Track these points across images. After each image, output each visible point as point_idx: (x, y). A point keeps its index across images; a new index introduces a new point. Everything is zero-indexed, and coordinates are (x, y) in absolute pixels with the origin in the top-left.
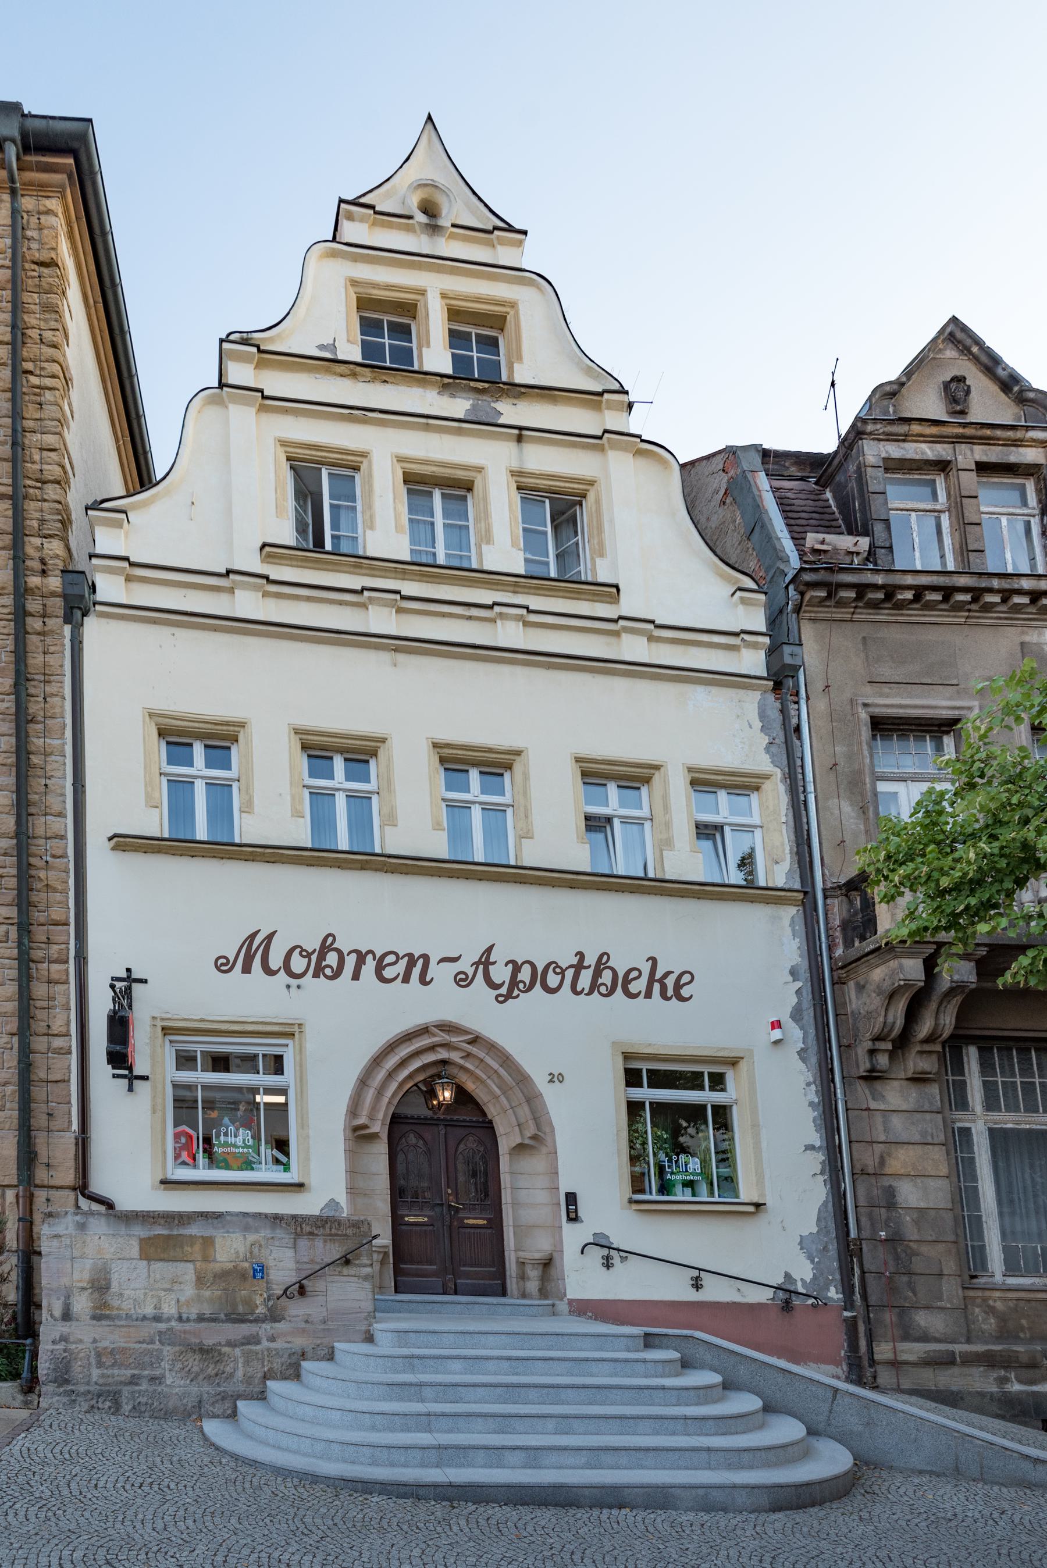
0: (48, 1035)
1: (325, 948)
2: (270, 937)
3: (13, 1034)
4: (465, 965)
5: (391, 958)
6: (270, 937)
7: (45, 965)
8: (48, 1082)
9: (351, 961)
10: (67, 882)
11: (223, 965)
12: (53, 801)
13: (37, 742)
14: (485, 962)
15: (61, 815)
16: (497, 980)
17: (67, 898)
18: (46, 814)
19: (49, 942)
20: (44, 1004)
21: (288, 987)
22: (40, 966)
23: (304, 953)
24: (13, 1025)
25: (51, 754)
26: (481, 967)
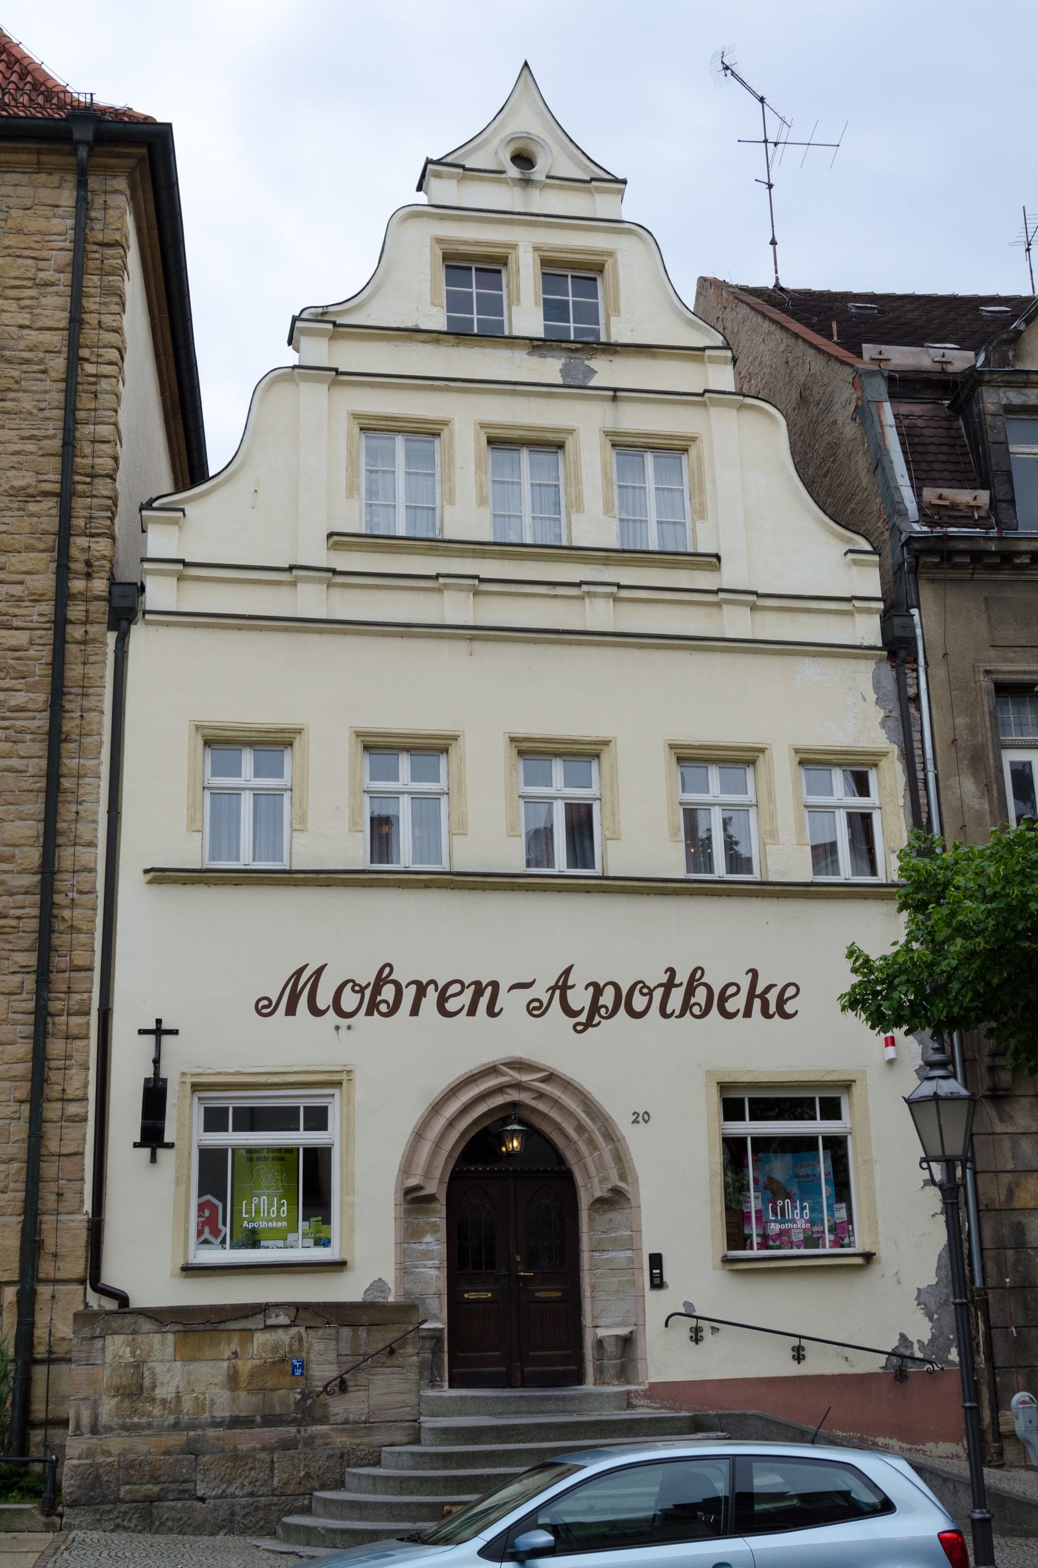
0: (63, 1100)
1: (380, 981)
2: (319, 972)
3: (21, 1102)
4: (539, 991)
5: (455, 988)
6: (319, 972)
7: (64, 1018)
8: (60, 1155)
9: (409, 995)
10: (93, 921)
11: (264, 1008)
12: (83, 829)
13: (70, 764)
14: (562, 986)
15: (92, 844)
16: (576, 1007)
17: (93, 939)
18: (75, 845)
19: (69, 991)
20: (60, 1064)
21: (337, 1028)
22: (57, 1019)
23: (357, 988)
24: (24, 1090)
25: (85, 776)
26: (558, 992)
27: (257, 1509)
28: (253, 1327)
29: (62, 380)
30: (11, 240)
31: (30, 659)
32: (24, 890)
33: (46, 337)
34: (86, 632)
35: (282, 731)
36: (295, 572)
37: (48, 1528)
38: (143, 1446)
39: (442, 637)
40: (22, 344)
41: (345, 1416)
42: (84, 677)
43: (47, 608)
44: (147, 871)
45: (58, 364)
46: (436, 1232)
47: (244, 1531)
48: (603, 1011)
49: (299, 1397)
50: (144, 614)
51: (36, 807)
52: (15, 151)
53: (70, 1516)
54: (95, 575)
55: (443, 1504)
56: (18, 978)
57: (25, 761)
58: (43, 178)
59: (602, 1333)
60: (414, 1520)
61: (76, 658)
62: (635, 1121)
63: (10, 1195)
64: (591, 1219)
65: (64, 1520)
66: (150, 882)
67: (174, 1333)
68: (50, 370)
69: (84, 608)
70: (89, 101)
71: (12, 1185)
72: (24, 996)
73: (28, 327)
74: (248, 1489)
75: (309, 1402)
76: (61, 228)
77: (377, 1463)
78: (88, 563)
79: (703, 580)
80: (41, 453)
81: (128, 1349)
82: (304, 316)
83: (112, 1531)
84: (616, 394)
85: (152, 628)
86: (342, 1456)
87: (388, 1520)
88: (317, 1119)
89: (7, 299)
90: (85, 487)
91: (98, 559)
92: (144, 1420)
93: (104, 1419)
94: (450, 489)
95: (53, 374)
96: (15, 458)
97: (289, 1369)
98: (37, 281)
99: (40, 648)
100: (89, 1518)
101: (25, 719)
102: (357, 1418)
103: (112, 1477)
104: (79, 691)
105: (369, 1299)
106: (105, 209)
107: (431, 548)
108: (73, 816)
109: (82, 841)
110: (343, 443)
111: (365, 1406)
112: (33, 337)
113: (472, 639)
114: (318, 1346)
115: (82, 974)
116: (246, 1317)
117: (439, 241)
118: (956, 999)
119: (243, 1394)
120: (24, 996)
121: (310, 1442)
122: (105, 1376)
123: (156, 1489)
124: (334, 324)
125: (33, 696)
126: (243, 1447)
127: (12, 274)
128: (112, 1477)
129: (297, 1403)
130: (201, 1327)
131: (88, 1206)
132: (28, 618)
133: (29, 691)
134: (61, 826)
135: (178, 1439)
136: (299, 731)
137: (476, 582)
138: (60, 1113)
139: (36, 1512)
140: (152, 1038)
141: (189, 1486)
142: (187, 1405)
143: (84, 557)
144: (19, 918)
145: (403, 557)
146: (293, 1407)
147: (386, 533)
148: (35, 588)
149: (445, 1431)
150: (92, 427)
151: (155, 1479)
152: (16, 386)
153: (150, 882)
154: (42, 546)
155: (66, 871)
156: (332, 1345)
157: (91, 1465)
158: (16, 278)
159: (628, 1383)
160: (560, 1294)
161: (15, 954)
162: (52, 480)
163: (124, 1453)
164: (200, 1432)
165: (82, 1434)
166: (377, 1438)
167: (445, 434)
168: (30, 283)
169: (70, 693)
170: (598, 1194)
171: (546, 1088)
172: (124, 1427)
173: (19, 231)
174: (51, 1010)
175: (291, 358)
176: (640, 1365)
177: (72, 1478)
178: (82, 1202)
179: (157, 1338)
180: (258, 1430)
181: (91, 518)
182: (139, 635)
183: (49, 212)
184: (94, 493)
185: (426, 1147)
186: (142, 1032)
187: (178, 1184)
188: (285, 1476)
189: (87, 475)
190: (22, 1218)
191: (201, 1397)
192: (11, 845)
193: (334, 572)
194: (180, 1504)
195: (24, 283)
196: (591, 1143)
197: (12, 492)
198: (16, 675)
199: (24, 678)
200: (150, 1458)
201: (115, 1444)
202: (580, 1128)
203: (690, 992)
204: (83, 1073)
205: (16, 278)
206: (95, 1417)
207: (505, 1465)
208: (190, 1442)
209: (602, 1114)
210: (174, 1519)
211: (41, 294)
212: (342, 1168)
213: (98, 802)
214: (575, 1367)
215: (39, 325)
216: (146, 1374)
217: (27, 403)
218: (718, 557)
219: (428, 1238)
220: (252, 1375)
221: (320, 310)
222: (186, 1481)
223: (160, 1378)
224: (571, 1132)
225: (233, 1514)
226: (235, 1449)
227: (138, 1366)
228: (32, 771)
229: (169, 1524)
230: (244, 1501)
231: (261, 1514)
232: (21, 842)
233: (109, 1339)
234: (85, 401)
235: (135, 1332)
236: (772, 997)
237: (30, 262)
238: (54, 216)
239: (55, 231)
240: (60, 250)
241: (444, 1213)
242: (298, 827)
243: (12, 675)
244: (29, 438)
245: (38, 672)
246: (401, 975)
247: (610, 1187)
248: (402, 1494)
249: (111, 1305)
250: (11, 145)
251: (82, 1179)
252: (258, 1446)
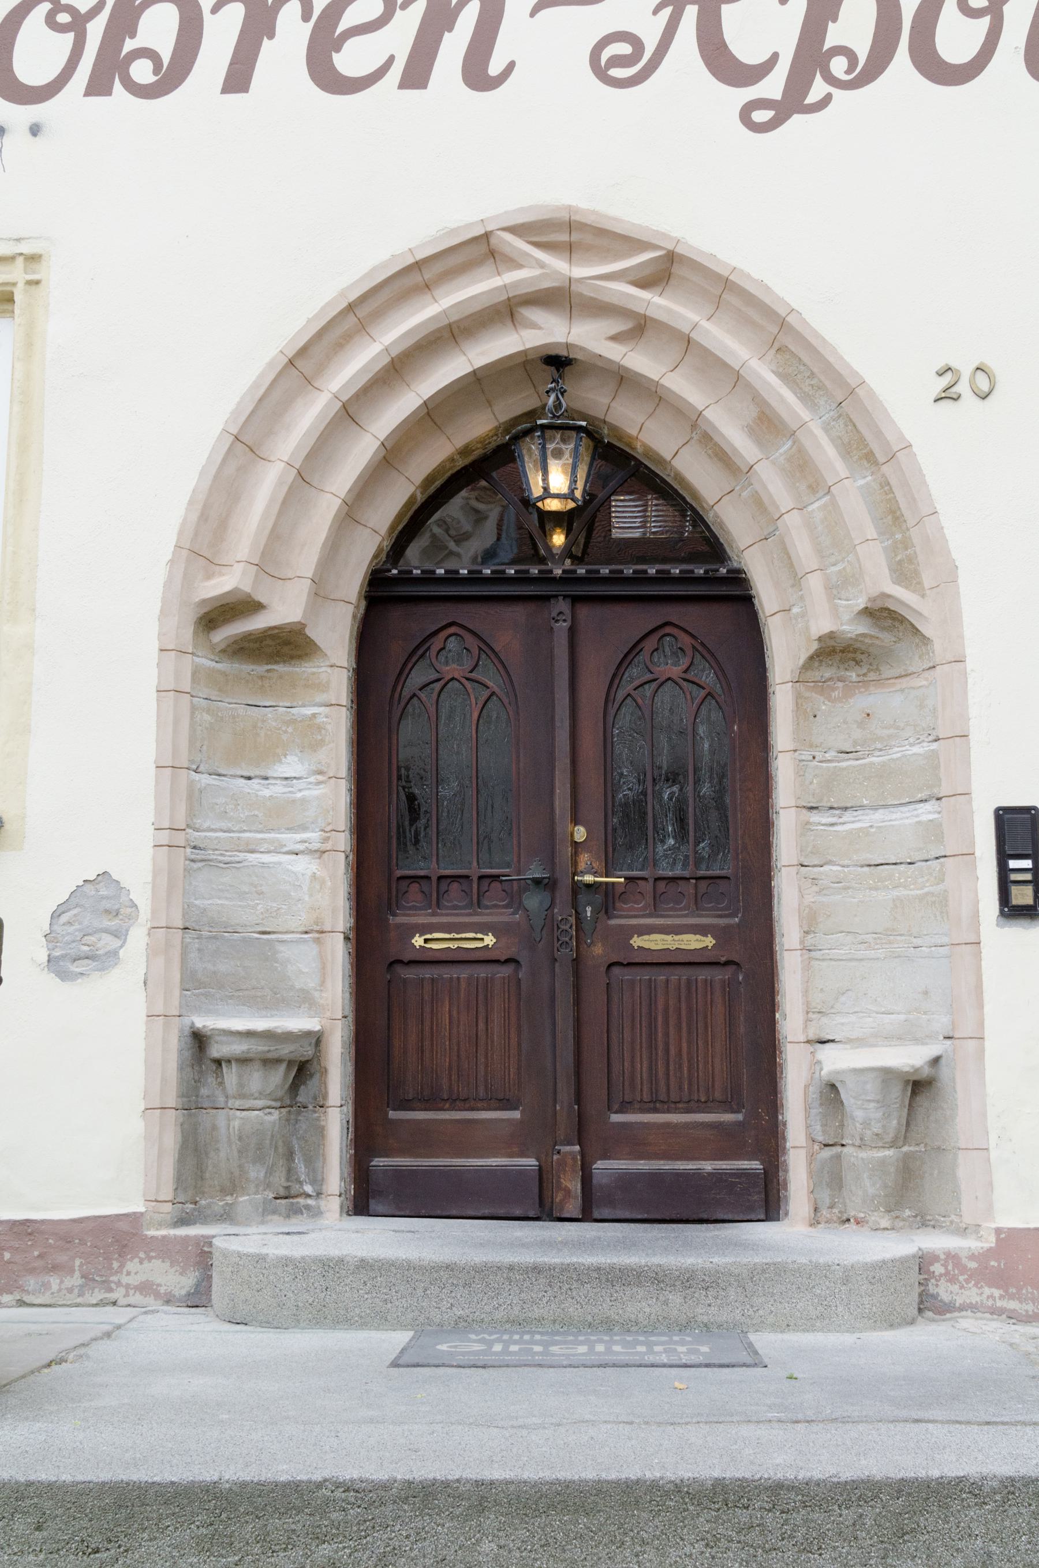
46: (315, 746)
48: (838, 66)
62: (948, 396)
64: (803, 713)
159: (924, 1221)
160: (709, 941)
170: (823, 625)
176: (966, 1168)
209: (839, 379)
219: (292, 765)
247: (861, 603)
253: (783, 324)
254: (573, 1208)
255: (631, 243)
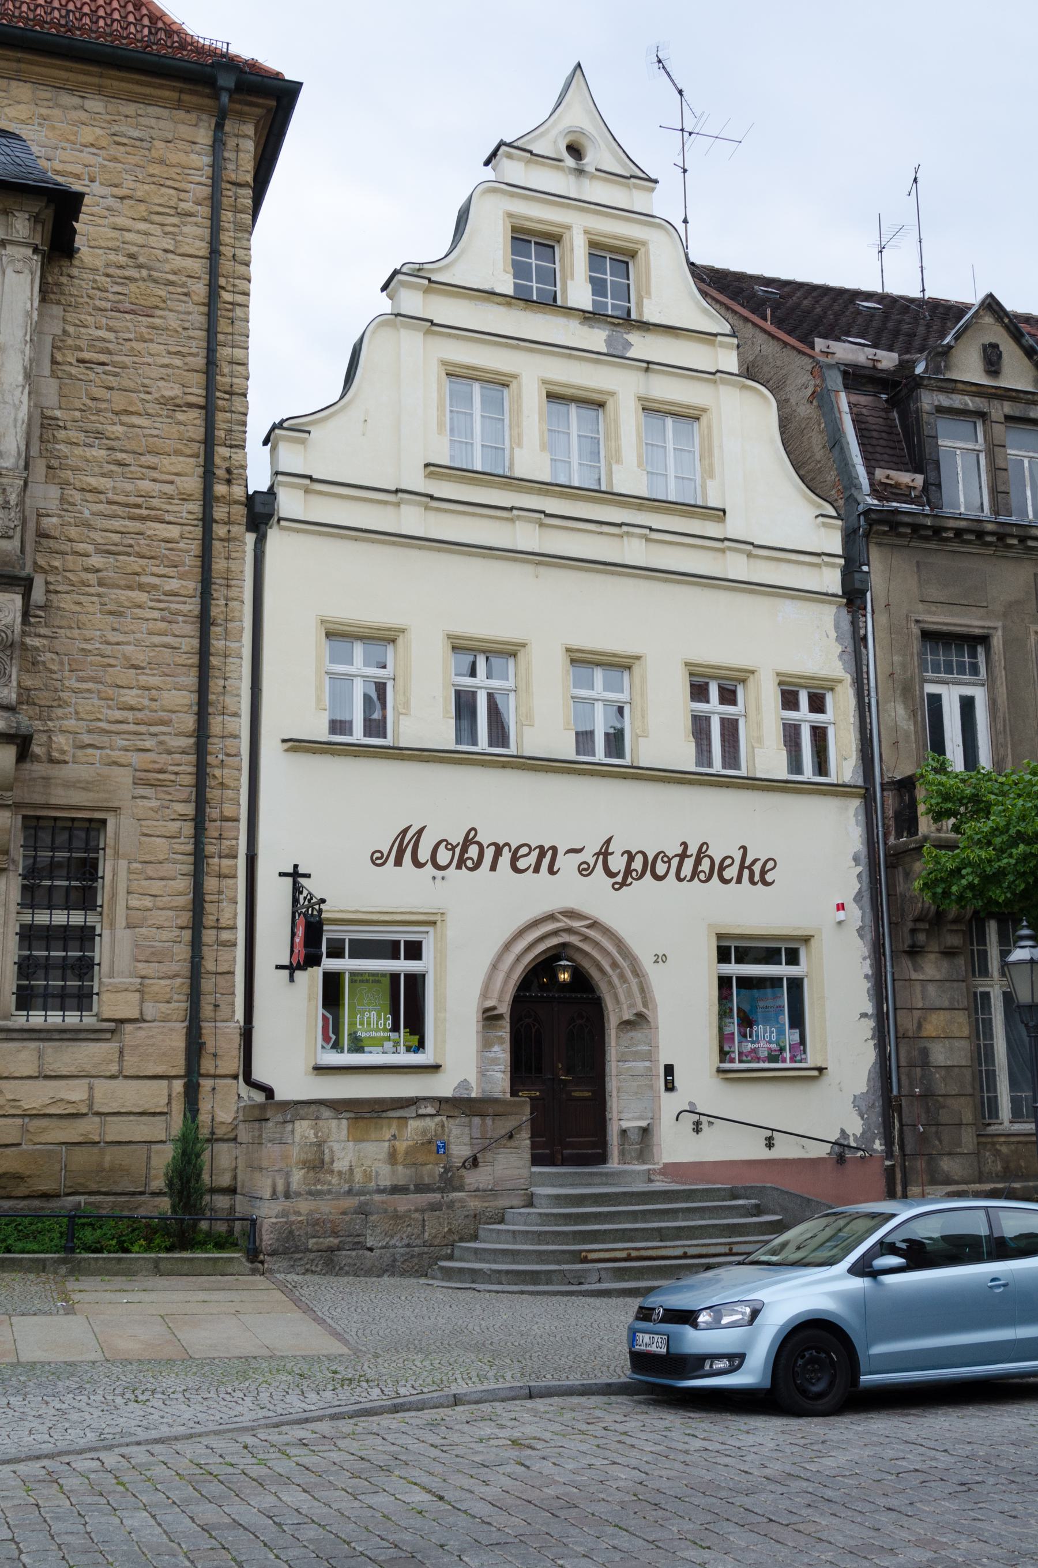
0: (218, 928)
1: (467, 842)
2: (420, 832)
3: (182, 928)
4: (588, 856)
5: (524, 850)
6: (420, 832)
7: (216, 860)
8: (216, 973)
9: (489, 853)
10: (239, 780)
11: (378, 859)
12: (229, 700)
13: (217, 644)
14: (604, 853)
15: (236, 715)
16: (614, 870)
17: (239, 794)
18: (223, 714)
19: (220, 837)
20: (215, 898)
21: (434, 878)
22: (210, 861)
23: (449, 847)
24: (185, 918)
25: (229, 656)
26: (601, 857)
27: (413, 1256)
28: (408, 1116)
29: (204, 304)
30: (154, 169)
31: (181, 551)
32: (181, 750)
33: (189, 263)
34: (229, 531)
35: (389, 629)
36: (400, 495)
37: (254, 1272)
38: (326, 1208)
39: (515, 560)
40: (167, 267)
41: (476, 1185)
42: (228, 570)
43: (196, 507)
44: (284, 741)
45: (200, 289)
46: (502, 1043)
47: (403, 1274)
48: (634, 874)
49: (442, 1170)
50: (279, 520)
51: (191, 679)
52: (161, 87)
53: (270, 1263)
54: (234, 482)
55: (581, 1251)
56: (178, 824)
57: (179, 640)
58: (181, 114)
59: (625, 1125)
60: (559, 1263)
61: (220, 553)
62: (656, 962)
63: (174, 1005)
64: (618, 1037)
65: (266, 1266)
66: (286, 750)
67: (347, 1119)
68: (192, 294)
69: (227, 510)
70: (225, 50)
71: (176, 997)
72: (182, 840)
73: (172, 252)
74: (406, 1241)
75: (450, 1174)
76: (199, 164)
77: (502, 1221)
78: (229, 471)
79: (711, 529)
80: (186, 368)
81: (312, 1132)
82: (404, 270)
83: (304, 1274)
84: (648, 366)
85: (285, 533)
86: (475, 1216)
87: (538, 1263)
88: (414, 951)
89: (152, 223)
90: (224, 402)
91: (237, 468)
92: (325, 1187)
93: (294, 1187)
94: (519, 434)
95: (195, 298)
96: (163, 370)
97: (435, 1148)
98: (179, 210)
99: (189, 542)
100: (285, 1264)
101: (178, 603)
102: (485, 1187)
103: (302, 1232)
104: (224, 582)
105: (457, 1095)
106: (237, 152)
107: (506, 484)
108: (220, 689)
109: (229, 712)
110: (435, 386)
111: (491, 1178)
112: (178, 262)
113: (539, 563)
114: (456, 1131)
115: (230, 824)
116: (402, 1108)
117: (510, 215)
118: (1009, 887)
119: (400, 1168)
120: (182, 840)
121: (451, 1205)
122: (295, 1153)
123: (336, 1241)
124: (429, 280)
125: (184, 583)
126: (401, 1209)
127: (157, 201)
128: (302, 1232)
129: (441, 1175)
130: (368, 1115)
131: (240, 1015)
132: (179, 515)
133: (180, 579)
134: (212, 697)
135: (351, 1202)
136: (403, 631)
137: (542, 516)
138: (214, 938)
139: (244, 1260)
140: (290, 880)
141: (361, 1239)
142: (358, 1176)
143: (226, 464)
144: (176, 773)
145: (471, 487)
146: (437, 1178)
147: (459, 466)
148: (184, 489)
149: (558, 1197)
150: (230, 349)
151: (335, 1234)
152: (162, 305)
153: (286, 750)
154: (188, 452)
155: (216, 736)
156: (467, 1130)
157: (286, 1223)
158: (160, 205)
159: (644, 1163)
161: (174, 804)
162: (197, 393)
163: (310, 1213)
164: (368, 1197)
165: (277, 1199)
166: (502, 1202)
167: (514, 385)
168: (172, 211)
169: (215, 584)
170: (626, 1017)
171: (591, 933)
172: (310, 1193)
173: (162, 162)
174: (207, 853)
175: (384, 305)
176: (655, 1149)
177: (272, 1232)
178: (234, 1012)
179: (334, 1123)
180: (412, 1196)
181: (231, 431)
182: (275, 538)
183: (187, 147)
184: (233, 409)
185: (500, 977)
186: (282, 874)
187: (310, 1000)
188: (434, 1231)
189: (226, 393)
190: (186, 1024)
191: (369, 1170)
192: (168, 711)
193: (432, 497)
194: (354, 1253)
195: (168, 210)
196: (622, 977)
197: (162, 401)
198: (170, 564)
199: (176, 567)
200: (331, 1217)
201: (304, 1206)
202: (615, 965)
203: (698, 862)
204: (233, 906)
205: (160, 205)
206: (288, 1185)
207: (609, 1223)
208: (361, 1205)
209: (632, 956)
210: (350, 1265)
211: (182, 223)
212: (436, 990)
213: (241, 679)
214: (600, 1151)
215: (181, 251)
216: (327, 1151)
217: (173, 321)
218: (724, 511)
219: (496, 1048)
220: (407, 1153)
221: (417, 266)
222: (358, 1236)
223: (338, 1154)
224: (608, 968)
225: (394, 1260)
226: (395, 1210)
227: (320, 1145)
228: (184, 648)
229: (346, 1268)
230: (402, 1250)
231: (416, 1260)
232: (177, 708)
233: (297, 1123)
234: (223, 325)
235: (317, 1118)
236: (757, 868)
237: (172, 192)
238: (192, 151)
239: (194, 166)
240: (198, 184)
241: (508, 1029)
242: (404, 711)
243: (166, 563)
244: (176, 353)
245: (188, 563)
246: (483, 838)
247: (635, 1011)
248: (540, 1244)
249: (259, 1097)
250: (158, 81)
251: (233, 994)
252: (413, 1208)
253: (620, 941)
254: (559, 1162)
255: (586, 918)
